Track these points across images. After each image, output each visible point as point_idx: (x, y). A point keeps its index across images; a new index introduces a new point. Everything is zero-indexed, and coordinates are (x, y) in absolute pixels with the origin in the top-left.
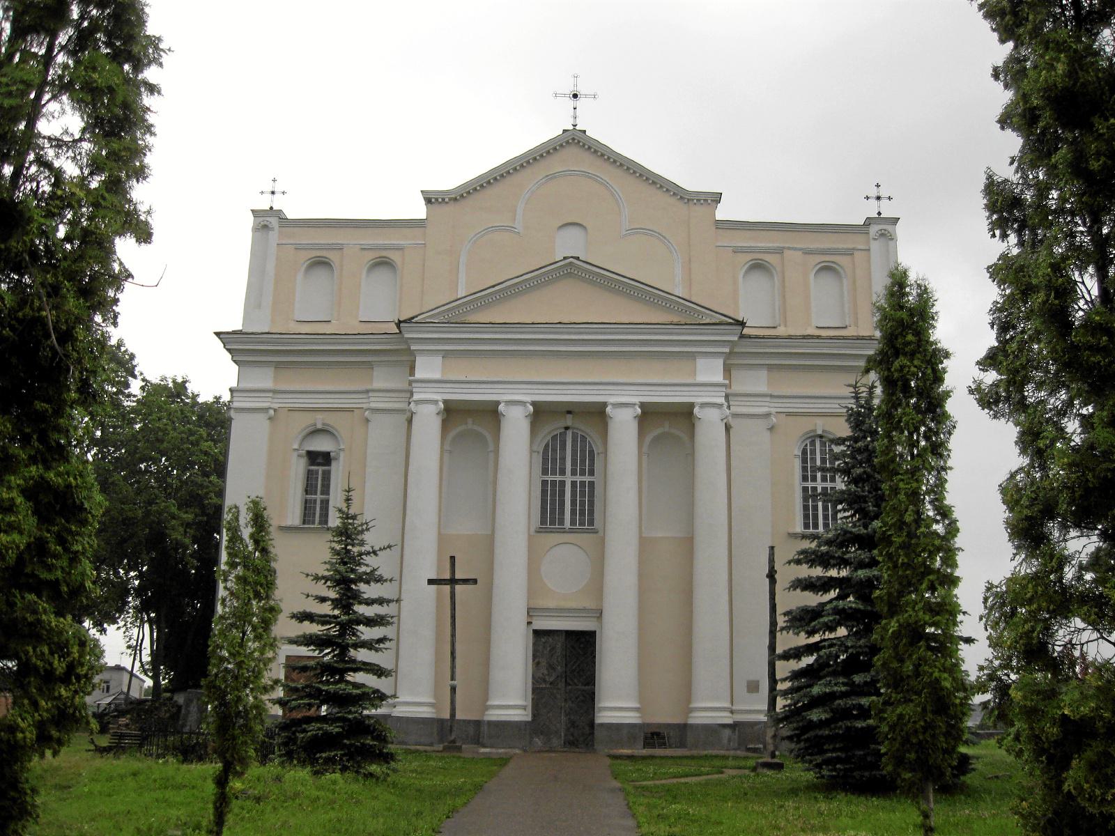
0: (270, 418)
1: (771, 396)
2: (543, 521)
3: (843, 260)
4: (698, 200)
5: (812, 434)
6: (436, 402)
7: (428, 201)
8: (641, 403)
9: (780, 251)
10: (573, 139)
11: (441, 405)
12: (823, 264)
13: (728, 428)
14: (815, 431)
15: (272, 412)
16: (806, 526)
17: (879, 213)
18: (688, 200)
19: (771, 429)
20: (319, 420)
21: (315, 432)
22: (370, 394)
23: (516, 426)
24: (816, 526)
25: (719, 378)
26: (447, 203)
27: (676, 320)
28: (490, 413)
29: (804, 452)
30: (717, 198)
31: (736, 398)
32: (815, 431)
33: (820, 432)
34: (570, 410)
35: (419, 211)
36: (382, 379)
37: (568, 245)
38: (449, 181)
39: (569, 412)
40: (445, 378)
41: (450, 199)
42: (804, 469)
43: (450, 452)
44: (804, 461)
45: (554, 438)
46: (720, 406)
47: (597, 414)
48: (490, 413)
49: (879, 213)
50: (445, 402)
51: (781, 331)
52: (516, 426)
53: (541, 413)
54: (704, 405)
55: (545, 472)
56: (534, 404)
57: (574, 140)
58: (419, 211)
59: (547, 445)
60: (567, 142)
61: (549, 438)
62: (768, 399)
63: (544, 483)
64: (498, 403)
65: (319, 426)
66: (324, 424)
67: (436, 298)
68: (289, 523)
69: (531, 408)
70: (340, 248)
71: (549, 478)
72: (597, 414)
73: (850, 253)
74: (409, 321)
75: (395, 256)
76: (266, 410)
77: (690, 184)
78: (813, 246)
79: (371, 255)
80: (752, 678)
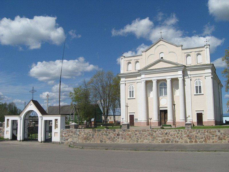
6: (144, 81)
9: (191, 52)
24: (198, 93)
25: (181, 73)
28: (151, 82)
34: (163, 80)
36: (138, 78)
40: (146, 77)
46: (181, 78)
47: (165, 80)
48: (151, 82)
51: (192, 65)
53: (158, 81)
54: (179, 78)
67: (144, 66)
72: (165, 80)
73: (202, 51)
76: (124, 83)
78: (196, 51)
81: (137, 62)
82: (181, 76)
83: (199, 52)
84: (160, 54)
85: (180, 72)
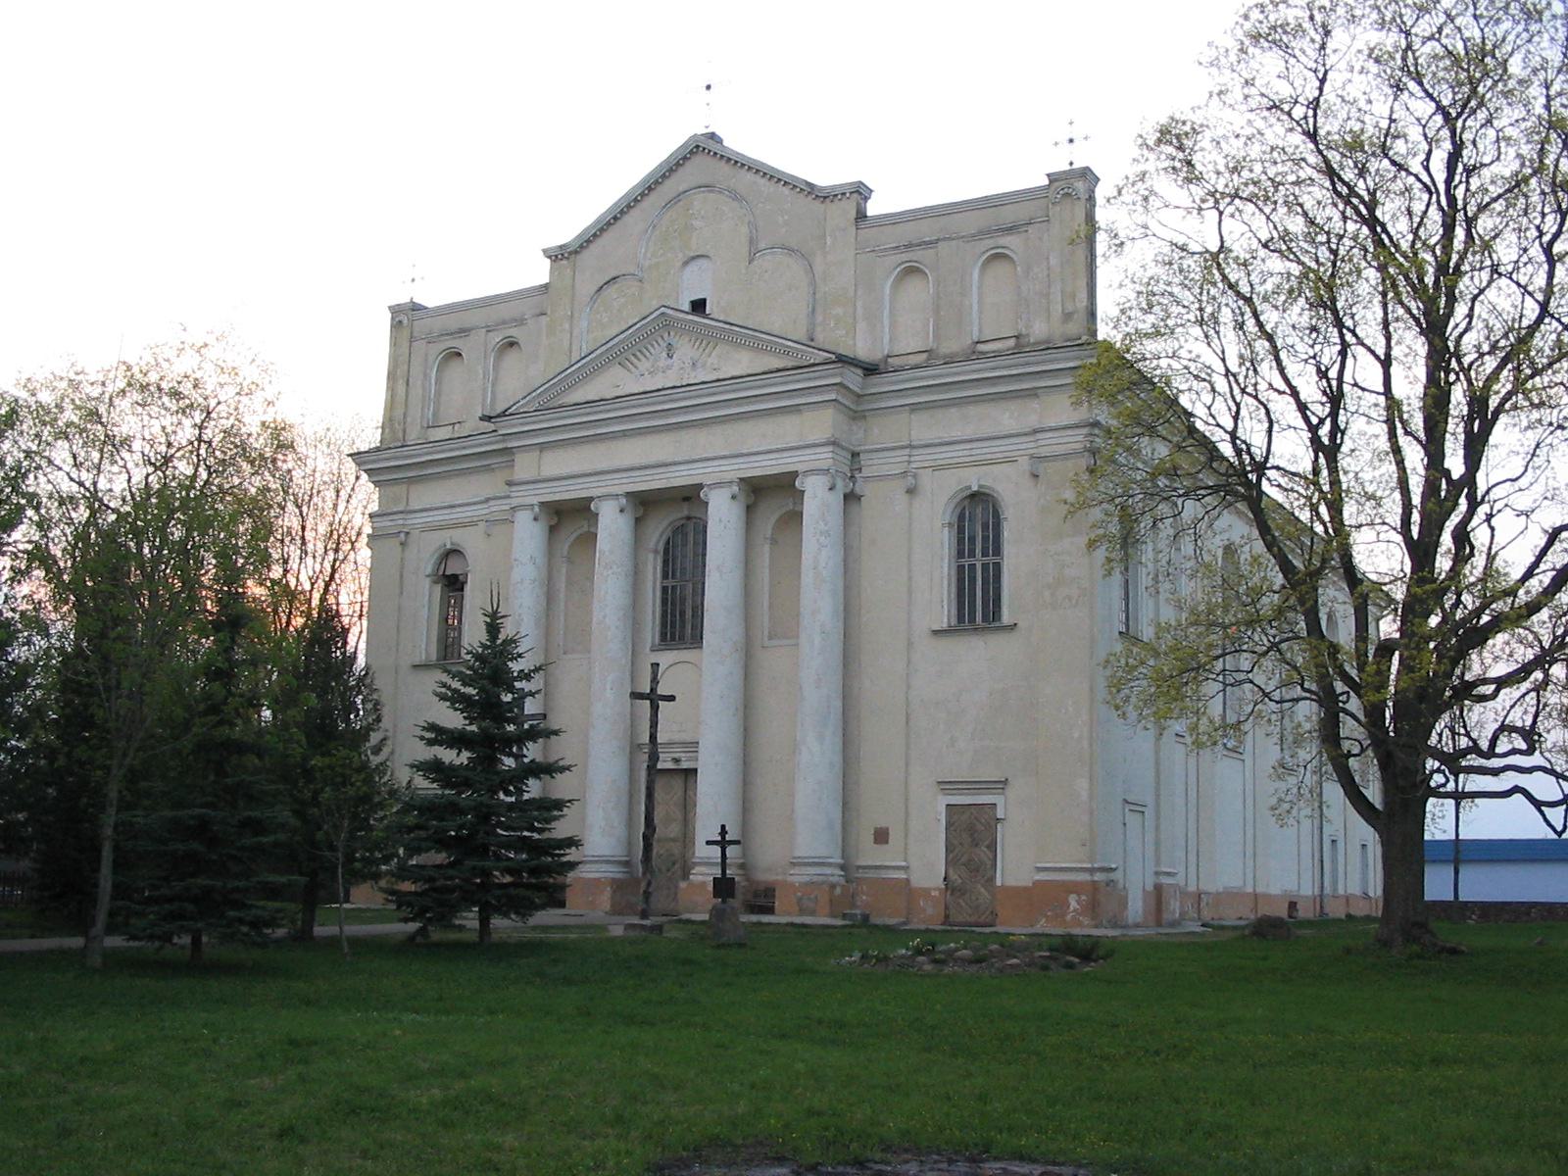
0: (401, 544)
1: (911, 447)
2: (663, 636)
3: (1011, 242)
4: (836, 195)
5: (968, 492)
7: (550, 257)
8: (741, 479)
10: (697, 147)
11: (537, 509)
12: (988, 254)
13: (851, 498)
14: (970, 487)
15: (402, 535)
16: (960, 618)
17: (1071, 164)
18: (825, 198)
19: (911, 491)
20: (447, 539)
21: (452, 553)
22: (492, 503)
23: (612, 525)
24: (972, 619)
26: (567, 258)
27: (781, 365)
29: (961, 518)
30: (860, 192)
31: (870, 456)
32: (970, 487)
33: (975, 488)
35: (540, 273)
37: (695, 283)
38: (567, 232)
39: (686, 499)
41: (570, 253)
42: (960, 541)
43: (570, 560)
44: (961, 530)
45: (675, 532)
47: (690, 496)
49: (1071, 164)
50: (542, 504)
52: (612, 525)
53: (644, 504)
55: (665, 576)
56: (628, 494)
57: (703, 149)
58: (540, 273)
59: (668, 543)
60: (691, 152)
61: (669, 533)
62: (907, 452)
63: (664, 589)
64: (591, 499)
65: (448, 546)
66: (452, 544)
68: (421, 657)
69: (624, 501)
70: (464, 332)
71: (670, 583)
74: (503, 414)
75: (513, 332)
77: (824, 177)
79: (497, 338)
80: (883, 825)
81: (512, 344)
82: (824, 457)
83: (990, 243)
84: (686, 263)
85: (821, 424)
